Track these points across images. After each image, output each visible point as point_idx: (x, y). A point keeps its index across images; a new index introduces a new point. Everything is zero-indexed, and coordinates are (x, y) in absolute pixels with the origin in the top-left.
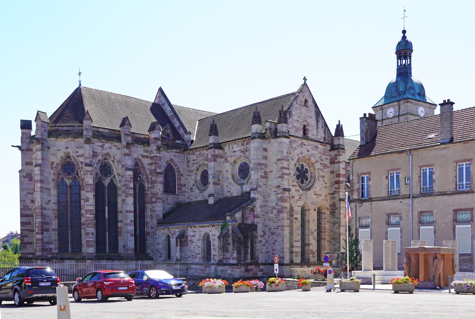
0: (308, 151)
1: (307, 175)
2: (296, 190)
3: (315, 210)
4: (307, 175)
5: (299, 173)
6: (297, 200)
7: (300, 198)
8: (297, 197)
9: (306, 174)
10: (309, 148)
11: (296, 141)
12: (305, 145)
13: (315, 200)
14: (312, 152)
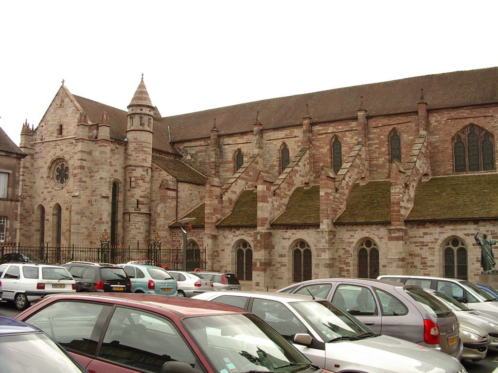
0: (62, 150)
1: (57, 174)
2: (48, 192)
3: (67, 209)
4: (57, 174)
5: (58, 174)
6: (49, 201)
7: (52, 199)
8: (49, 199)
9: (58, 174)
10: (63, 147)
11: (50, 144)
12: (58, 145)
13: (67, 199)
14: (65, 149)
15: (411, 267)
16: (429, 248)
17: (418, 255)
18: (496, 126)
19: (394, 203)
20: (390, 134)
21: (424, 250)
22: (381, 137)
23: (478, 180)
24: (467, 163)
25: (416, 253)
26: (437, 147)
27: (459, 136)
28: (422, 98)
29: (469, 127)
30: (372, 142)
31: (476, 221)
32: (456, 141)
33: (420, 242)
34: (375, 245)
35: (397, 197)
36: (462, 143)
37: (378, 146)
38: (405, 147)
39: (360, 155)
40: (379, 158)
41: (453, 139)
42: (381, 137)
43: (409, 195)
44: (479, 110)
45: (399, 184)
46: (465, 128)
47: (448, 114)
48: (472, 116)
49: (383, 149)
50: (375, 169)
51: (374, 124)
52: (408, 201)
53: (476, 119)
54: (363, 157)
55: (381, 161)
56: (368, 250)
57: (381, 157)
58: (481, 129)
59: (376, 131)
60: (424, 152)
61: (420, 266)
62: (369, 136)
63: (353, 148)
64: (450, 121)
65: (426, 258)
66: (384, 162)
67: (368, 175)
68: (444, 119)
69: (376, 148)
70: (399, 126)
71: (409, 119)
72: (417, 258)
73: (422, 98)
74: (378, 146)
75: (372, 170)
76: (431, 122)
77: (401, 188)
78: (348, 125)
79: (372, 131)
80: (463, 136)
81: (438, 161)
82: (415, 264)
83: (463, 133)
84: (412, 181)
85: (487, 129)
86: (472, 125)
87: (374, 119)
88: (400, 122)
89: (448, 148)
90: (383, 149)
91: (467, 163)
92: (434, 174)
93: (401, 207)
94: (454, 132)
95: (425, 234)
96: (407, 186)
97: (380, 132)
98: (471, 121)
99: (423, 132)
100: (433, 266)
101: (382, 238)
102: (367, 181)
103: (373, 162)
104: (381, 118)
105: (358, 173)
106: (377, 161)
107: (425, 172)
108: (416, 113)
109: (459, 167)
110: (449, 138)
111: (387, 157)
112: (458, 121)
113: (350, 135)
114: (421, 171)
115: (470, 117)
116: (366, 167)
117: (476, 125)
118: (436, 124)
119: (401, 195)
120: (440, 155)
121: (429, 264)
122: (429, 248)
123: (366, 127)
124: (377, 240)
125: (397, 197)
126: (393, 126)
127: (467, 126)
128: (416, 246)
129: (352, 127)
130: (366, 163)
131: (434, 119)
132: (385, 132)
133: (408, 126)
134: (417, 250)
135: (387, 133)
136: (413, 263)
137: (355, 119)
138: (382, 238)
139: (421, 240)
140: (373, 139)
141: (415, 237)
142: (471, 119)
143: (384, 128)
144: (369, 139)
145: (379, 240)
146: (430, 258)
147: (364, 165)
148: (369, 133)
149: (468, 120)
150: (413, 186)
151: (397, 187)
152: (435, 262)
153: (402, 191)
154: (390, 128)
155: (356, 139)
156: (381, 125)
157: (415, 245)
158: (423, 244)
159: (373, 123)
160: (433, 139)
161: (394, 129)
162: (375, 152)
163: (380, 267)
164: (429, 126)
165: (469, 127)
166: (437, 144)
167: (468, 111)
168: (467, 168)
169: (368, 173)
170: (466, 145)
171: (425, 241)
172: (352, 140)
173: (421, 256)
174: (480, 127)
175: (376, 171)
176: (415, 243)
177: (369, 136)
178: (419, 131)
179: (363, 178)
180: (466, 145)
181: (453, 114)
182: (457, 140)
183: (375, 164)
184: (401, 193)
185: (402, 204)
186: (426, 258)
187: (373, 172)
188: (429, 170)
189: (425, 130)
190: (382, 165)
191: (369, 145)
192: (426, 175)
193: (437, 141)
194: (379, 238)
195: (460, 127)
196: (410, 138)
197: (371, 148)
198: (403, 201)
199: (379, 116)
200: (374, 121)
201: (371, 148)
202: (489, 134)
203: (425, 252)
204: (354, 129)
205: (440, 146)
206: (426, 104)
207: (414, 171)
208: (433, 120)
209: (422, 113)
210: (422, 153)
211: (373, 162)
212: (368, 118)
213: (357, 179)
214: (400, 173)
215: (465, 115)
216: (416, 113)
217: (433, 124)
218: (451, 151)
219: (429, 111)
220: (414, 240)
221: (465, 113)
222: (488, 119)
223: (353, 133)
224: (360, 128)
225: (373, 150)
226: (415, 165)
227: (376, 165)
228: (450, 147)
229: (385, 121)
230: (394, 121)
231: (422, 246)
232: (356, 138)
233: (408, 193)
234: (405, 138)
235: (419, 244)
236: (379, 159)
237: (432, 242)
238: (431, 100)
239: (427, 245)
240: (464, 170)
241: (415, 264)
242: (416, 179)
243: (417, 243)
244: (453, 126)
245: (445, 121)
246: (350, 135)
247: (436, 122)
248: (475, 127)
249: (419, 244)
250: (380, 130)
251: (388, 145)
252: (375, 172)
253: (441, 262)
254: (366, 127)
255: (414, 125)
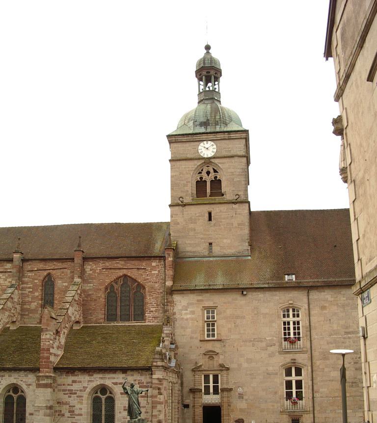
15: (58, 415)
16: (77, 397)
17: (66, 403)
18: (148, 279)
19: (43, 349)
20: (44, 279)
21: (72, 398)
22: (35, 281)
23: (128, 330)
24: (119, 313)
25: (64, 401)
26: (90, 295)
27: (112, 286)
28: (79, 246)
29: (122, 278)
30: (25, 285)
31: (124, 370)
32: (109, 291)
33: (69, 390)
34: (22, 392)
35: (48, 343)
36: (116, 293)
37: (31, 290)
38: (59, 293)
39: (12, 298)
40: (31, 302)
41: (106, 288)
42: (35, 281)
43: (60, 342)
44: (133, 262)
45: (50, 330)
46: (118, 278)
47: (103, 263)
48: (126, 268)
49: (37, 294)
50: (27, 313)
51: (29, 267)
52: (58, 347)
53: (130, 270)
54: (16, 300)
55: (33, 305)
56: (15, 396)
57: (35, 302)
58: (135, 281)
59: (30, 274)
60: (77, 299)
61: (67, 414)
62: (24, 279)
63: (5, 290)
64: (104, 270)
65: (74, 406)
66: (37, 307)
67: (19, 319)
68: (98, 268)
69: (29, 292)
70: (54, 272)
71: (65, 265)
72: (64, 406)
73: (79, 246)
74: (31, 290)
75: (24, 315)
76: (86, 270)
77: (52, 334)
78: (2, 266)
79: (26, 275)
80: (116, 286)
81: (90, 309)
82: (62, 412)
83: (116, 283)
84: (64, 328)
85: (140, 281)
86: (125, 276)
87: (30, 263)
88: (56, 268)
89: (101, 297)
90: (37, 294)
91: (119, 313)
92: (85, 322)
93: (51, 354)
94: (108, 281)
95: (74, 382)
96: (58, 332)
97: (34, 276)
98: (125, 272)
99: (77, 280)
100: (81, 415)
101: (30, 385)
102: (18, 325)
103: (25, 306)
104: (37, 261)
105: (9, 316)
106: (29, 305)
107: (77, 320)
108: (72, 260)
109: (111, 317)
110: (103, 287)
111: (40, 302)
112: (113, 271)
113: (4, 277)
114: (73, 319)
115: (122, 268)
116: (18, 311)
117: (129, 277)
118: (91, 272)
119: (51, 342)
120: (93, 304)
121: (77, 412)
122: (77, 397)
123: (21, 270)
124: (24, 387)
125: (48, 343)
126: (48, 271)
127: (121, 277)
128: (64, 394)
129: (7, 269)
130: (18, 307)
131: (90, 267)
132: (40, 276)
133: (63, 273)
134: (65, 398)
135: (42, 278)
136: (61, 411)
137: (11, 261)
138: (30, 385)
139: (69, 388)
140: (27, 283)
141: (64, 385)
142: (124, 270)
143: (39, 273)
144: (23, 283)
145: (26, 387)
146: (78, 406)
147: (16, 308)
148: (23, 276)
149: (122, 270)
150: (64, 332)
151: (48, 333)
152: (83, 410)
153: (52, 338)
154: (45, 273)
155: (9, 282)
156: (36, 269)
157: (63, 392)
158: (72, 392)
159: (28, 266)
160: (88, 287)
161: (49, 274)
162: (28, 296)
163: (27, 415)
164: (84, 274)
165: (122, 278)
166: (90, 293)
167: (123, 263)
168: (118, 318)
169: (19, 317)
170: (119, 295)
171: (74, 389)
172: (6, 282)
173: (69, 404)
174: (132, 279)
175: (28, 315)
176: (64, 390)
177: (24, 279)
178: (73, 278)
179: (13, 322)
180: (119, 295)
181: (108, 264)
182: (110, 290)
183: (27, 308)
184: (51, 340)
185: (52, 351)
186: (74, 406)
187: (24, 317)
188: (81, 318)
189: (79, 277)
190: (34, 310)
191: (23, 289)
192: (78, 322)
193: (91, 289)
194: (27, 385)
195: (114, 277)
196: (64, 284)
197: (24, 292)
198: (53, 348)
199: (35, 260)
200: (30, 265)
201: (24, 292)
202: (141, 286)
203: (73, 400)
204: (8, 270)
205: (93, 294)
206: (83, 252)
207: (66, 318)
208: (89, 267)
209: (78, 260)
210: (75, 301)
211: (25, 306)
212: (24, 261)
213: (7, 323)
214: (52, 319)
215: (120, 266)
216: (72, 260)
217: (87, 272)
218: (104, 300)
219: (85, 259)
220: (63, 387)
221: (120, 264)
222: (141, 272)
223: (7, 274)
224: (14, 271)
225: (26, 294)
226: (67, 311)
227: (28, 310)
228: (103, 296)
229: (41, 265)
230: (50, 266)
231: (70, 394)
232: (10, 280)
233: (59, 340)
234: (60, 284)
235: (67, 392)
236: (32, 304)
237: (81, 391)
238: (89, 249)
239: (76, 393)
240: (115, 320)
241: (62, 412)
242: (67, 326)
243: (66, 390)
244: (107, 276)
245: (100, 270)
246: (4, 277)
247: (91, 270)
248: (129, 278)
249: (67, 392)
250: (35, 274)
251: (42, 289)
252: (26, 317)
253: (89, 410)
254: (21, 270)
255: (69, 271)
